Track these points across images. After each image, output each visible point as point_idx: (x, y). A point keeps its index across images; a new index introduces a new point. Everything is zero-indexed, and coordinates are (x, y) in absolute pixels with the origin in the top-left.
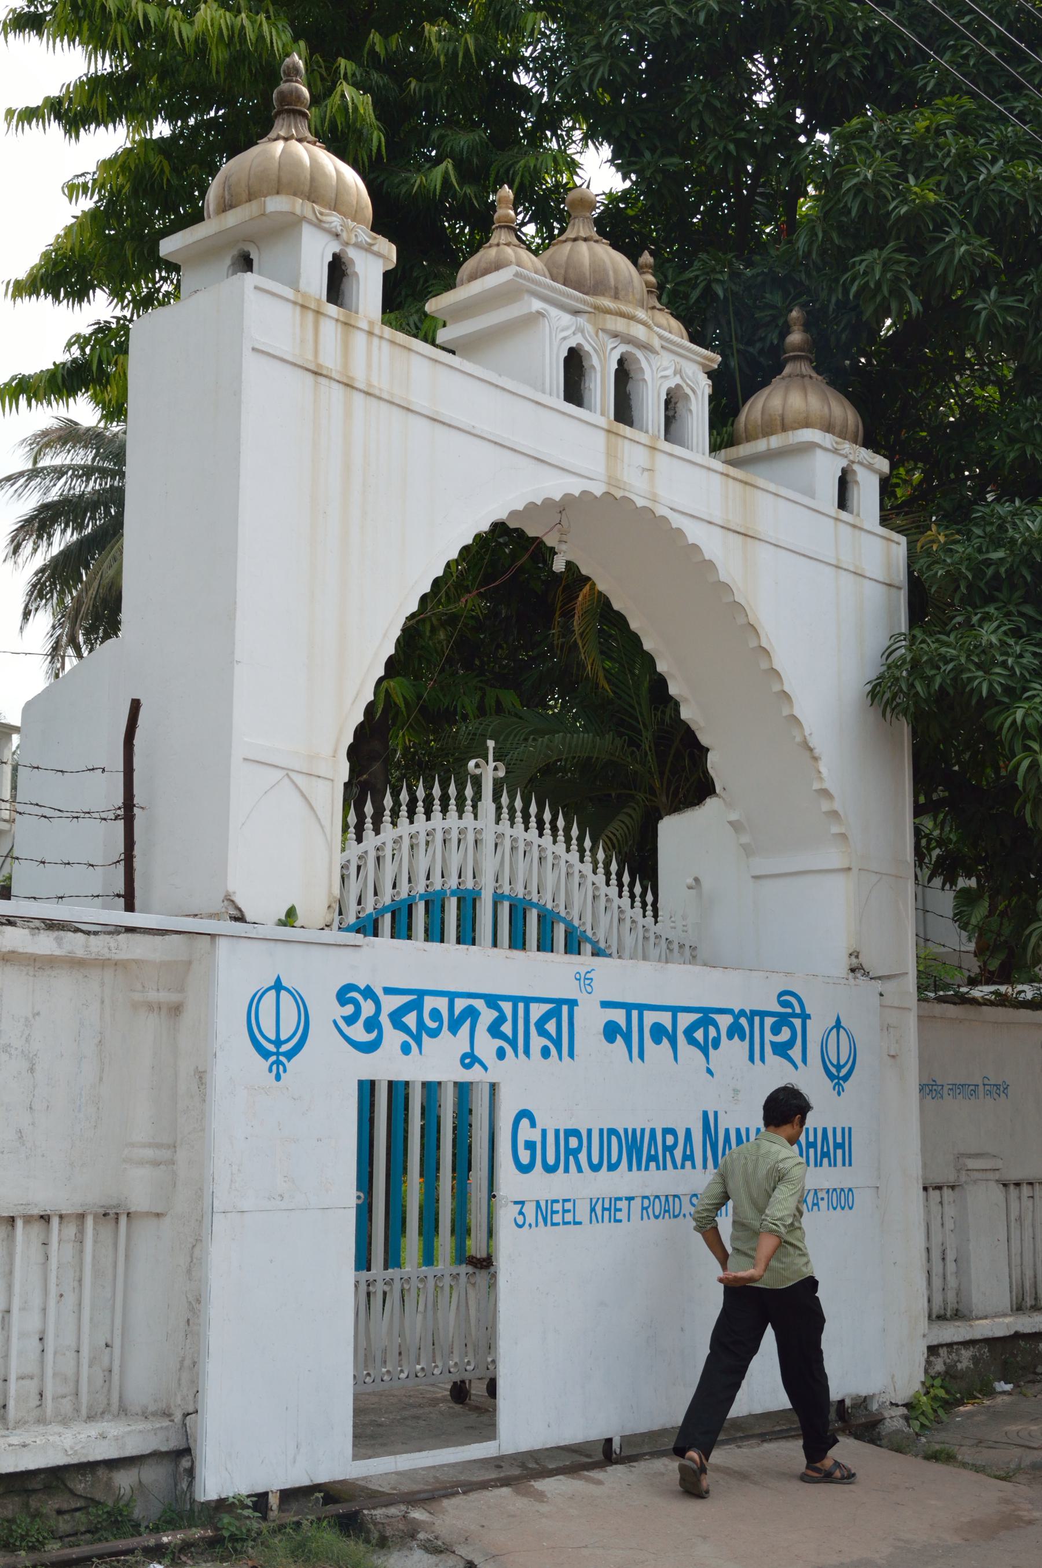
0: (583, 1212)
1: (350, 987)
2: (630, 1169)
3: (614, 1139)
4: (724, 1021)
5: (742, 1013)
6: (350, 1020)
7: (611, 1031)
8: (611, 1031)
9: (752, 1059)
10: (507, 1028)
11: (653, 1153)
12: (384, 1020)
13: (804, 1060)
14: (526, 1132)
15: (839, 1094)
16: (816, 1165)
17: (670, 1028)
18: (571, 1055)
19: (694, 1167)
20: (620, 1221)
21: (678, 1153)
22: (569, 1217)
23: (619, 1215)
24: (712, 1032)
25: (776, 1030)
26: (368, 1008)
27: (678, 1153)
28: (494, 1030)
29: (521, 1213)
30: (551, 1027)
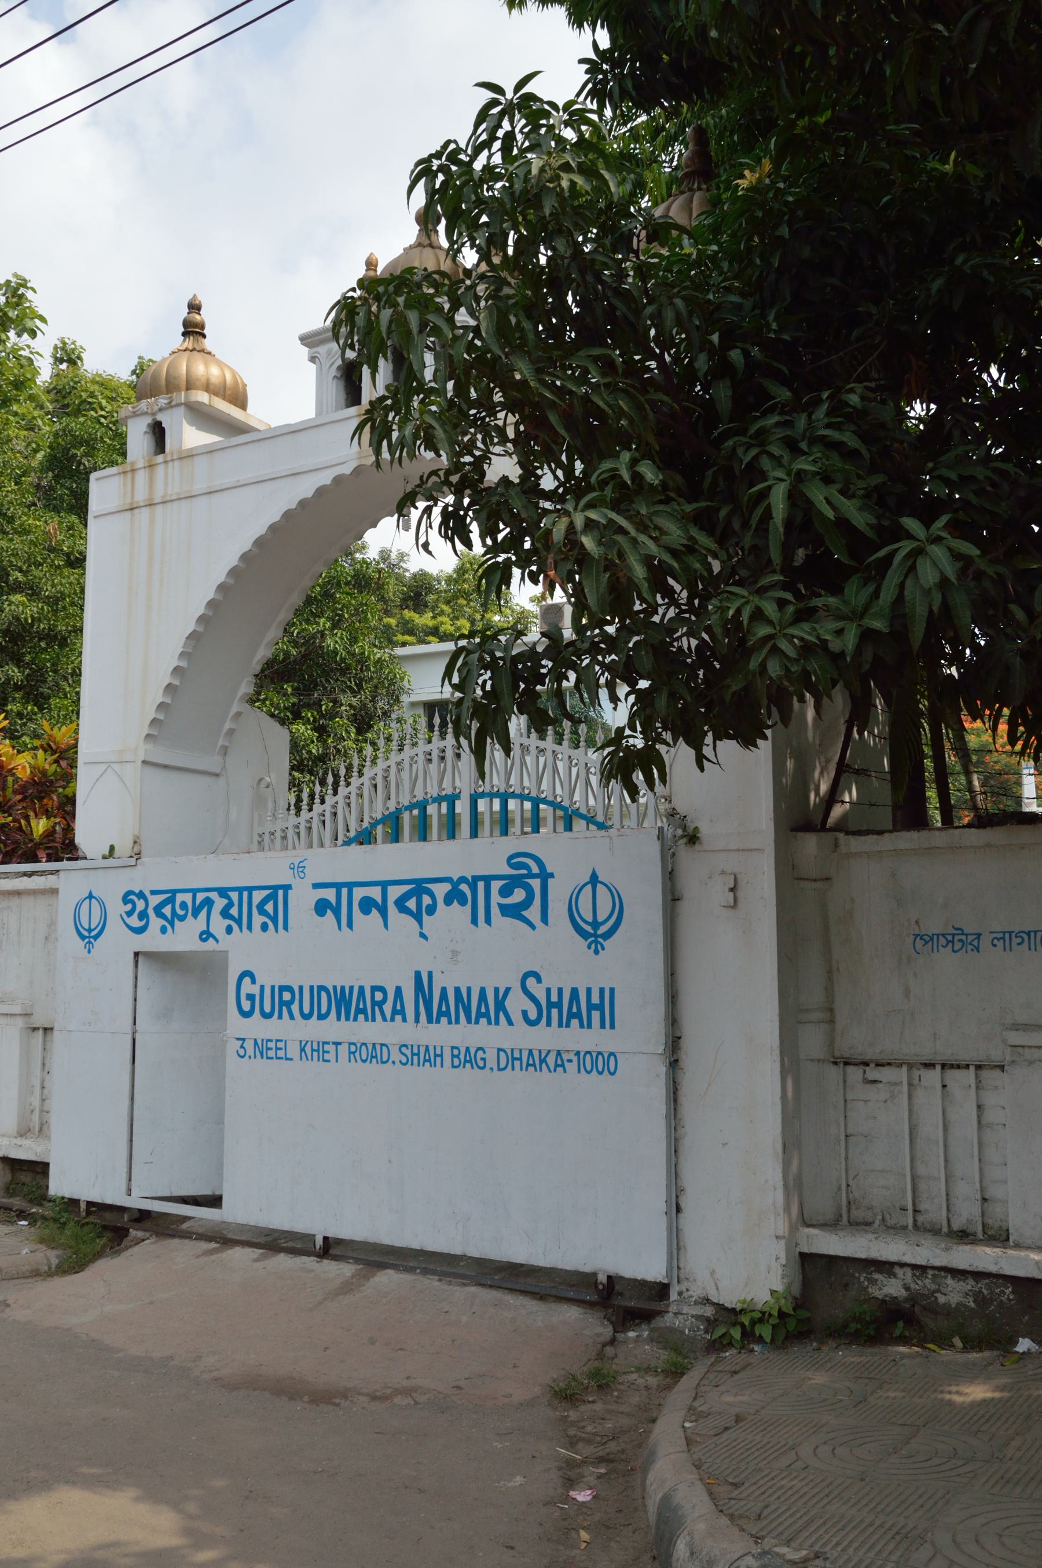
0: (293, 1051)
1: (130, 893)
2: (339, 1019)
3: (324, 994)
4: (441, 890)
5: (463, 880)
6: (129, 914)
7: (321, 908)
8: (321, 908)
9: (474, 921)
10: (234, 911)
11: (361, 1006)
12: (151, 912)
13: (545, 919)
14: (247, 987)
15: (596, 952)
16: (560, 1025)
17: (379, 900)
18: (286, 928)
19: (404, 1020)
20: (329, 1061)
21: (388, 1008)
22: (281, 1054)
23: (327, 1056)
24: (426, 900)
25: (505, 892)
26: (140, 905)
27: (388, 1008)
28: (225, 913)
29: (242, 1047)
30: (269, 907)
